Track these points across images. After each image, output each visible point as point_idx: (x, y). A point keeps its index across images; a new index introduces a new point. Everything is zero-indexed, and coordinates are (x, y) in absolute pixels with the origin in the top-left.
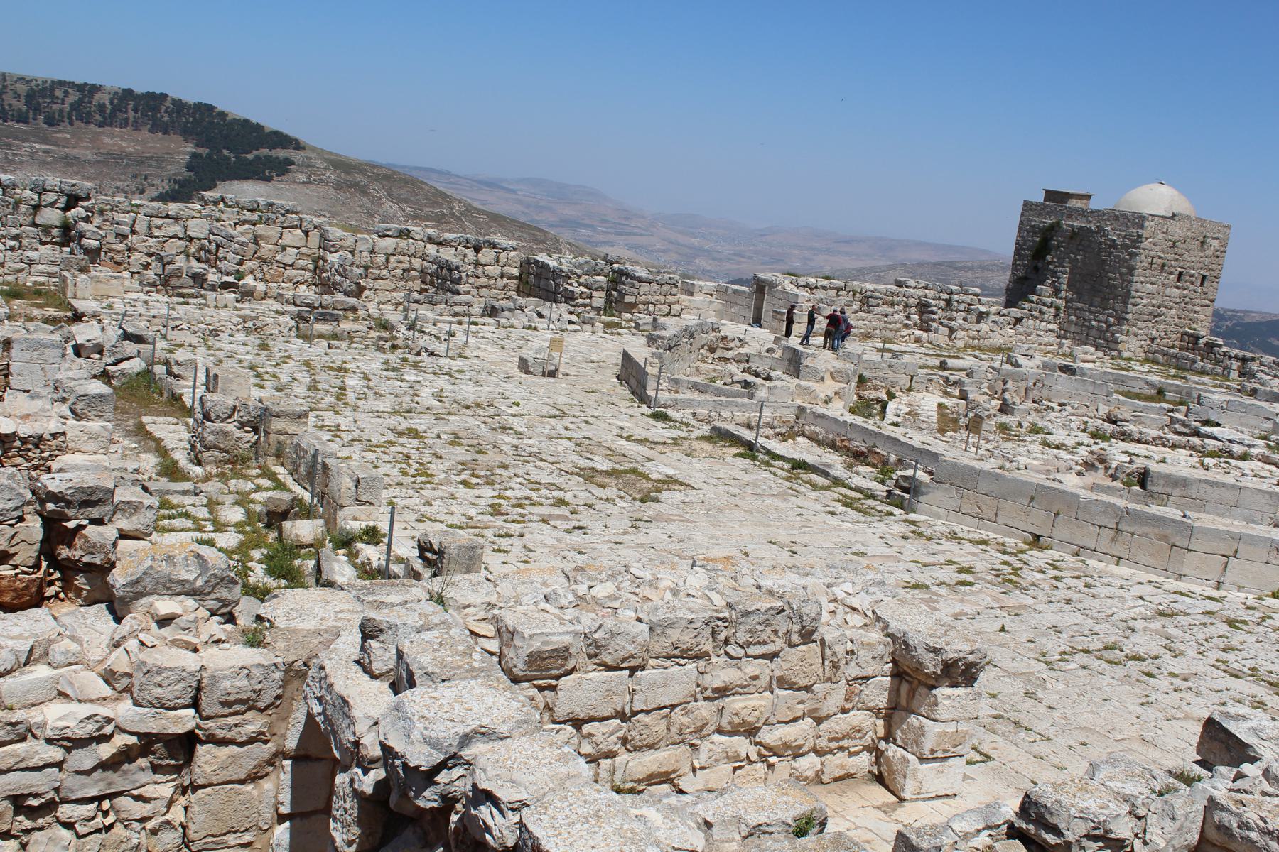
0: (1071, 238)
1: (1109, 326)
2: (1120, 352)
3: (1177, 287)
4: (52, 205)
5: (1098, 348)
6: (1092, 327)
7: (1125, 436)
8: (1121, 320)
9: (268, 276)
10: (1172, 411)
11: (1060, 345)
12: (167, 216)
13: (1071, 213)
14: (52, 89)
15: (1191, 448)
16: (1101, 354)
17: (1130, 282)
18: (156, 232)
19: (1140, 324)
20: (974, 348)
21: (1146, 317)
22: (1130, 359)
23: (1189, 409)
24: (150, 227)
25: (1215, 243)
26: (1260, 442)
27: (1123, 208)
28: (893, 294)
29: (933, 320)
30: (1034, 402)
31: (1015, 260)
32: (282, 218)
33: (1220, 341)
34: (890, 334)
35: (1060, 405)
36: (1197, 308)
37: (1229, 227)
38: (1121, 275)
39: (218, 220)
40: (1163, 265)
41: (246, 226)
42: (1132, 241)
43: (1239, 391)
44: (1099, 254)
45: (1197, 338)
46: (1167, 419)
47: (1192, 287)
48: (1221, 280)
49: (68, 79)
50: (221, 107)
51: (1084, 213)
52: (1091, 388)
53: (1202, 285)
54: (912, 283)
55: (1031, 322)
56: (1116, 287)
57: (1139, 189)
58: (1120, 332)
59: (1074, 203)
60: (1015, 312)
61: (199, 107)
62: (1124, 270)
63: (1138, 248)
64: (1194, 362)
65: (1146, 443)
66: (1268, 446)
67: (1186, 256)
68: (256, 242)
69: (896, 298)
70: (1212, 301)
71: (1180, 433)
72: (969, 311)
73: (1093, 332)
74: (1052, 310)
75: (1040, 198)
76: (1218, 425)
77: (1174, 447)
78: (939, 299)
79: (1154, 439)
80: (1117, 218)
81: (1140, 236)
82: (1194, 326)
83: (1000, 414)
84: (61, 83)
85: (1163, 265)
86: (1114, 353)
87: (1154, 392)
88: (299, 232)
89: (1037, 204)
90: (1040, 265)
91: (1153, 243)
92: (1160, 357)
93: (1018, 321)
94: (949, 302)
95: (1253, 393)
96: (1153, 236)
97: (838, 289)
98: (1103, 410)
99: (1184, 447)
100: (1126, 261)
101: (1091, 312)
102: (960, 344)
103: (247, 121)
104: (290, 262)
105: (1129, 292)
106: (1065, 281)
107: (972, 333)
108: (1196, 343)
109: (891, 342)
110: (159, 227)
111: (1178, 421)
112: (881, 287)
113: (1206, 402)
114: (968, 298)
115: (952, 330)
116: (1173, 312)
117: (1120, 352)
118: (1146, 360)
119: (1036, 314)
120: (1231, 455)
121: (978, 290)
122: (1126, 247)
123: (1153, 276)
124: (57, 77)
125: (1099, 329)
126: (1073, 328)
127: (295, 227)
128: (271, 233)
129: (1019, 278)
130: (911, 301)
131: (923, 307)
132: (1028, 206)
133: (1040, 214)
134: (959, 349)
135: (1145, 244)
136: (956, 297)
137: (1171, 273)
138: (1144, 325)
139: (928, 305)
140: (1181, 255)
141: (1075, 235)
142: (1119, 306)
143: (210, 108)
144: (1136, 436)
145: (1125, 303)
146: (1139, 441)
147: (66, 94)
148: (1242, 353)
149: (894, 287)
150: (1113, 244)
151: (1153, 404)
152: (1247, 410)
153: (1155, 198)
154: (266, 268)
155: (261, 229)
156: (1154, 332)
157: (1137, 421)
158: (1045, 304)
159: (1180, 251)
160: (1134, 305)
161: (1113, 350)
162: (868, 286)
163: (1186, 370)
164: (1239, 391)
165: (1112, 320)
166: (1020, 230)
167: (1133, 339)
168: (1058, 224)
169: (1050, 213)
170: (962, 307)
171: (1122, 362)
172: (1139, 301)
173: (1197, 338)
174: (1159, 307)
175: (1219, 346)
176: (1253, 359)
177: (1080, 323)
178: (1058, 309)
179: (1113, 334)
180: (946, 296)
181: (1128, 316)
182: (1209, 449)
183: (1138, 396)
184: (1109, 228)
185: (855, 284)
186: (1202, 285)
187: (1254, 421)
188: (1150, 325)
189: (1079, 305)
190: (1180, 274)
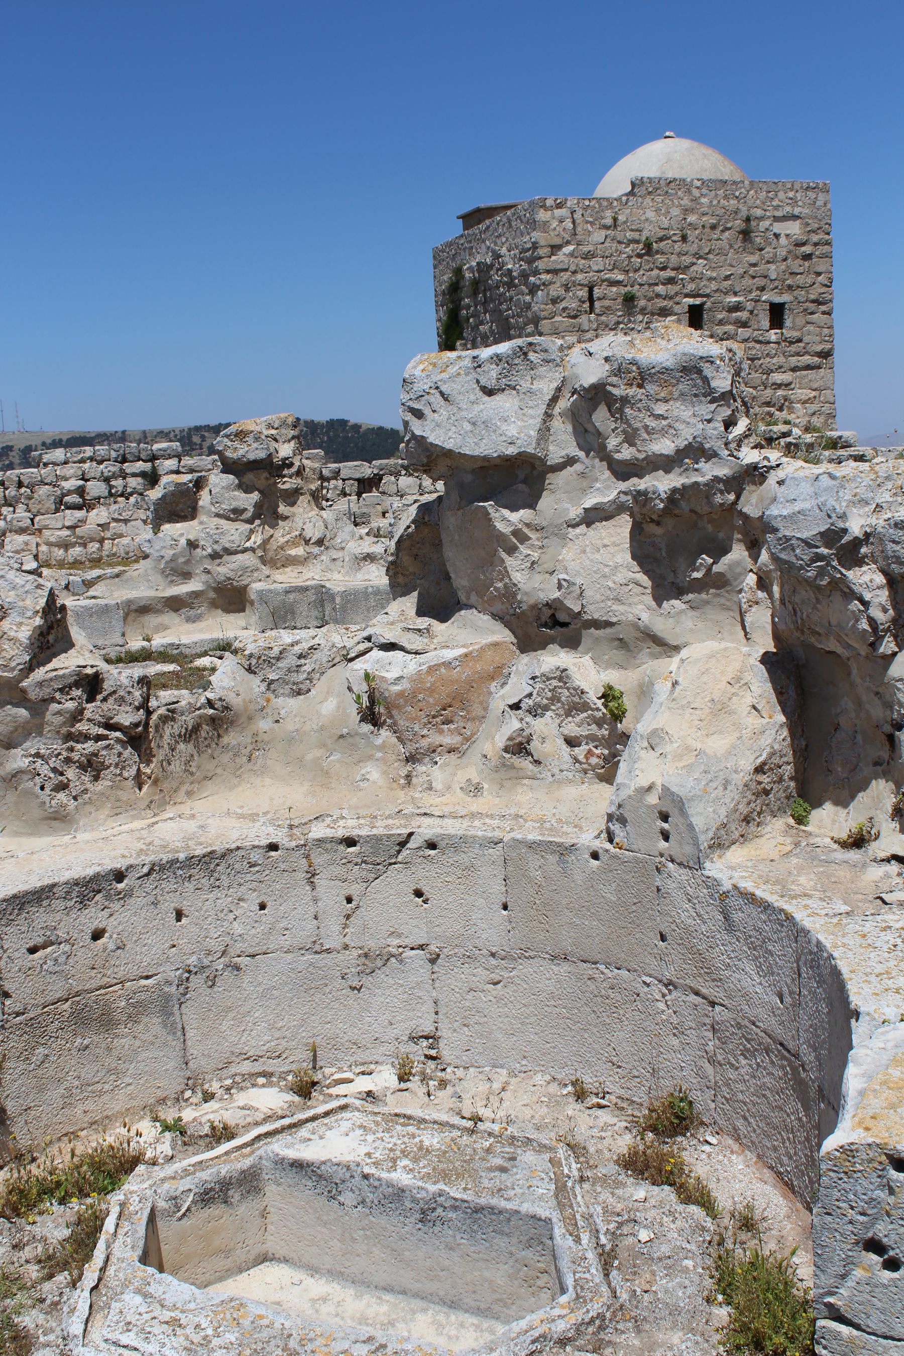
14: (189, 436)
36: (777, 377)
40: (629, 300)
42: (530, 261)
49: (203, 423)
50: (353, 420)
61: (332, 424)
70: (826, 355)
78: (124, 475)
81: (535, 246)
84: (197, 429)
85: (629, 300)
103: (381, 428)
124: (192, 424)
143: (343, 423)
147: (203, 438)
159: (674, 260)
180: (140, 466)
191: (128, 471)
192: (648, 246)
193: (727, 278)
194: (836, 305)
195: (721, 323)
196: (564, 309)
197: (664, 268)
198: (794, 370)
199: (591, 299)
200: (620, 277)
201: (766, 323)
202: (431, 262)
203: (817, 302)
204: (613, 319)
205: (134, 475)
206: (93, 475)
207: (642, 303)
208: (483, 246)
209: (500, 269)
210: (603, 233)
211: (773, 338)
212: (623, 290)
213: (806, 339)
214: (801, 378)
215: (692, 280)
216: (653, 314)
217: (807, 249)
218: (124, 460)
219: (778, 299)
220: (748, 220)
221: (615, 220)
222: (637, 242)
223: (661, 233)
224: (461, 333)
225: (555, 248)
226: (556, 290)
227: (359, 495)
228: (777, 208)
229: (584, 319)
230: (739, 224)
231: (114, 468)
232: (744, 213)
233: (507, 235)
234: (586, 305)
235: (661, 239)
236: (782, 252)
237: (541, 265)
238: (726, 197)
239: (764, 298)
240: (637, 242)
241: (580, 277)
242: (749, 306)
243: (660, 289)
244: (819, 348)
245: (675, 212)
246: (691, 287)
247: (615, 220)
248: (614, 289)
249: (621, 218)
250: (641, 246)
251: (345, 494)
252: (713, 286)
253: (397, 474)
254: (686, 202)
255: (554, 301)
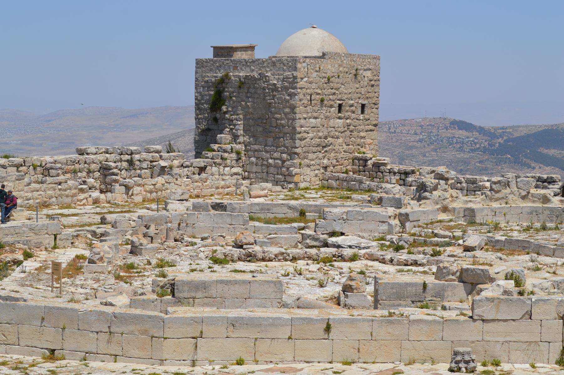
0: (240, 87)
1: (284, 162)
2: (296, 184)
3: (340, 118)
5: (276, 183)
6: (269, 166)
7: (250, 257)
8: (292, 155)
10: (303, 229)
11: (238, 186)
13: (236, 65)
15: (309, 258)
16: (279, 188)
17: (294, 119)
19: (311, 156)
20: (152, 201)
21: (314, 149)
22: (307, 189)
23: (316, 225)
25: (368, 74)
26: (375, 244)
27: (283, 54)
28: (74, 162)
29: (116, 181)
30: (176, 240)
31: (197, 115)
33: (387, 160)
34: (68, 200)
35: (203, 239)
36: (362, 134)
37: (377, 58)
38: (285, 114)
40: (322, 101)
42: (290, 83)
43: (369, 202)
44: (264, 99)
45: (366, 161)
46: (299, 237)
47: (353, 116)
48: (380, 106)
51: (246, 64)
52: (229, 220)
53: (363, 112)
54: (92, 149)
55: (215, 169)
56: (283, 126)
57: (294, 35)
58: (293, 166)
59: (238, 56)
60: (200, 162)
62: (287, 110)
63: (295, 88)
64: (361, 182)
65: (270, 260)
66: (383, 245)
67: (342, 89)
69: (77, 166)
71: (312, 247)
72: (152, 167)
73: (272, 170)
74: (234, 156)
75: (209, 54)
76: (342, 234)
77: (294, 259)
78: (121, 161)
79: (276, 255)
80: (274, 64)
81: (295, 78)
82: (363, 150)
83: (130, 256)
85: (322, 101)
86: (291, 186)
87: (297, 214)
89: (207, 61)
90: (218, 116)
91: (308, 82)
92: (334, 183)
93: (202, 170)
94: (131, 162)
95: (380, 201)
96: (307, 75)
97: (18, 166)
98: (230, 239)
99: (303, 258)
100: (288, 101)
101: (267, 152)
102: (138, 199)
105: (294, 128)
106: (241, 127)
107: (148, 188)
108: (365, 166)
109: (69, 207)
111: (309, 236)
112: (61, 158)
113: (329, 217)
114: (149, 156)
115: (128, 188)
116: (341, 140)
117: (296, 184)
118: (323, 187)
119: (218, 161)
120: (342, 258)
121: (159, 147)
122: (286, 88)
123: (314, 111)
125: (275, 166)
126: (254, 169)
129: (203, 131)
130: (93, 166)
131: (105, 170)
132: (200, 63)
133: (211, 70)
134: (136, 205)
135: (301, 84)
136: (137, 157)
137: (331, 106)
138: (314, 156)
139: (108, 168)
140: (337, 89)
141: (242, 84)
142: (288, 143)
144: (260, 256)
145: (293, 139)
146: (263, 260)
148: (403, 168)
149: (75, 156)
150: (275, 88)
151: (285, 226)
152: (363, 217)
153: (309, 41)
156: (325, 161)
157: (273, 242)
158: (225, 151)
159: (336, 86)
160: (301, 140)
161: (290, 183)
162: (48, 159)
163: (355, 191)
164: (369, 202)
165: (284, 156)
166: (197, 86)
167: (307, 171)
168: (227, 76)
169: (219, 68)
170: (145, 165)
171: (297, 192)
172: (305, 135)
173: (366, 161)
174: (326, 138)
175: (385, 165)
176: (413, 172)
177: (260, 162)
178: (238, 153)
179: (288, 169)
180: (127, 157)
181: (297, 150)
182: (321, 256)
183: (281, 221)
184: (269, 74)
185: (35, 158)
186: (363, 112)
187: (372, 226)
188: (321, 155)
189: (256, 147)
190: (340, 106)
191: (123, 159)
192: (329, 79)
193: (350, 93)
194: (379, 105)
195: (347, 111)
196: (303, 104)
197: (332, 89)
198: (366, 131)
199: (311, 100)
200: (320, 92)
201: (360, 112)
202: (194, 65)
203: (375, 104)
204: (317, 108)
205: (125, 161)
206: (111, 160)
207: (325, 102)
208: (248, 69)
209: (266, 82)
210: (316, 73)
211: (362, 118)
212: (321, 97)
213: (371, 119)
214: (368, 134)
215: (340, 93)
216: (328, 107)
217: (373, 82)
218: (121, 154)
219: (364, 103)
220: (357, 70)
221: (320, 68)
222: (325, 78)
223: (332, 75)
224: (224, 103)
225: (302, 79)
226: (301, 96)
227: (199, 174)
228: (365, 65)
229: (308, 108)
230: (354, 72)
231: (118, 158)
232: (355, 68)
233: (272, 68)
234: (309, 102)
235: (332, 77)
236: (366, 84)
237: (298, 85)
238: (351, 61)
239: (360, 102)
240: (325, 78)
241: (308, 91)
242: (356, 105)
243: (331, 97)
244: (374, 123)
245: (336, 66)
246: (340, 96)
247: (320, 68)
248: (318, 96)
249: (322, 68)
250: (326, 79)
251: (194, 174)
252: (346, 96)
253: (212, 166)
254: (339, 62)
255: (300, 100)
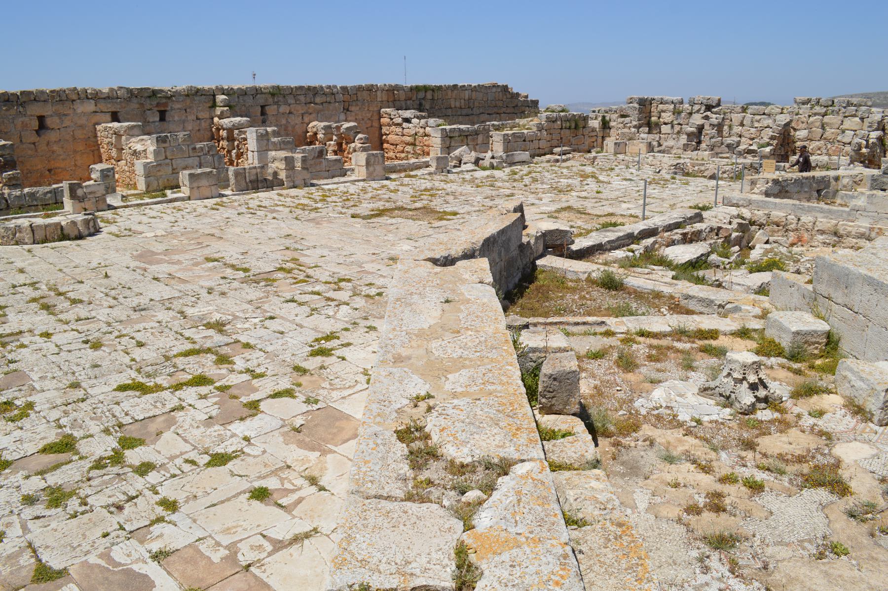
4: (698, 111)
9: (830, 152)
12: (764, 114)
18: (756, 124)
24: (752, 122)
32: (843, 110)
39: (797, 114)
41: (817, 117)
68: (823, 128)
88: (857, 119)
104: (848, 141)
110: (758, 121)
127: (854, 116)
128: (835, 121)
154: (829, 146)
155: (826, 119)
